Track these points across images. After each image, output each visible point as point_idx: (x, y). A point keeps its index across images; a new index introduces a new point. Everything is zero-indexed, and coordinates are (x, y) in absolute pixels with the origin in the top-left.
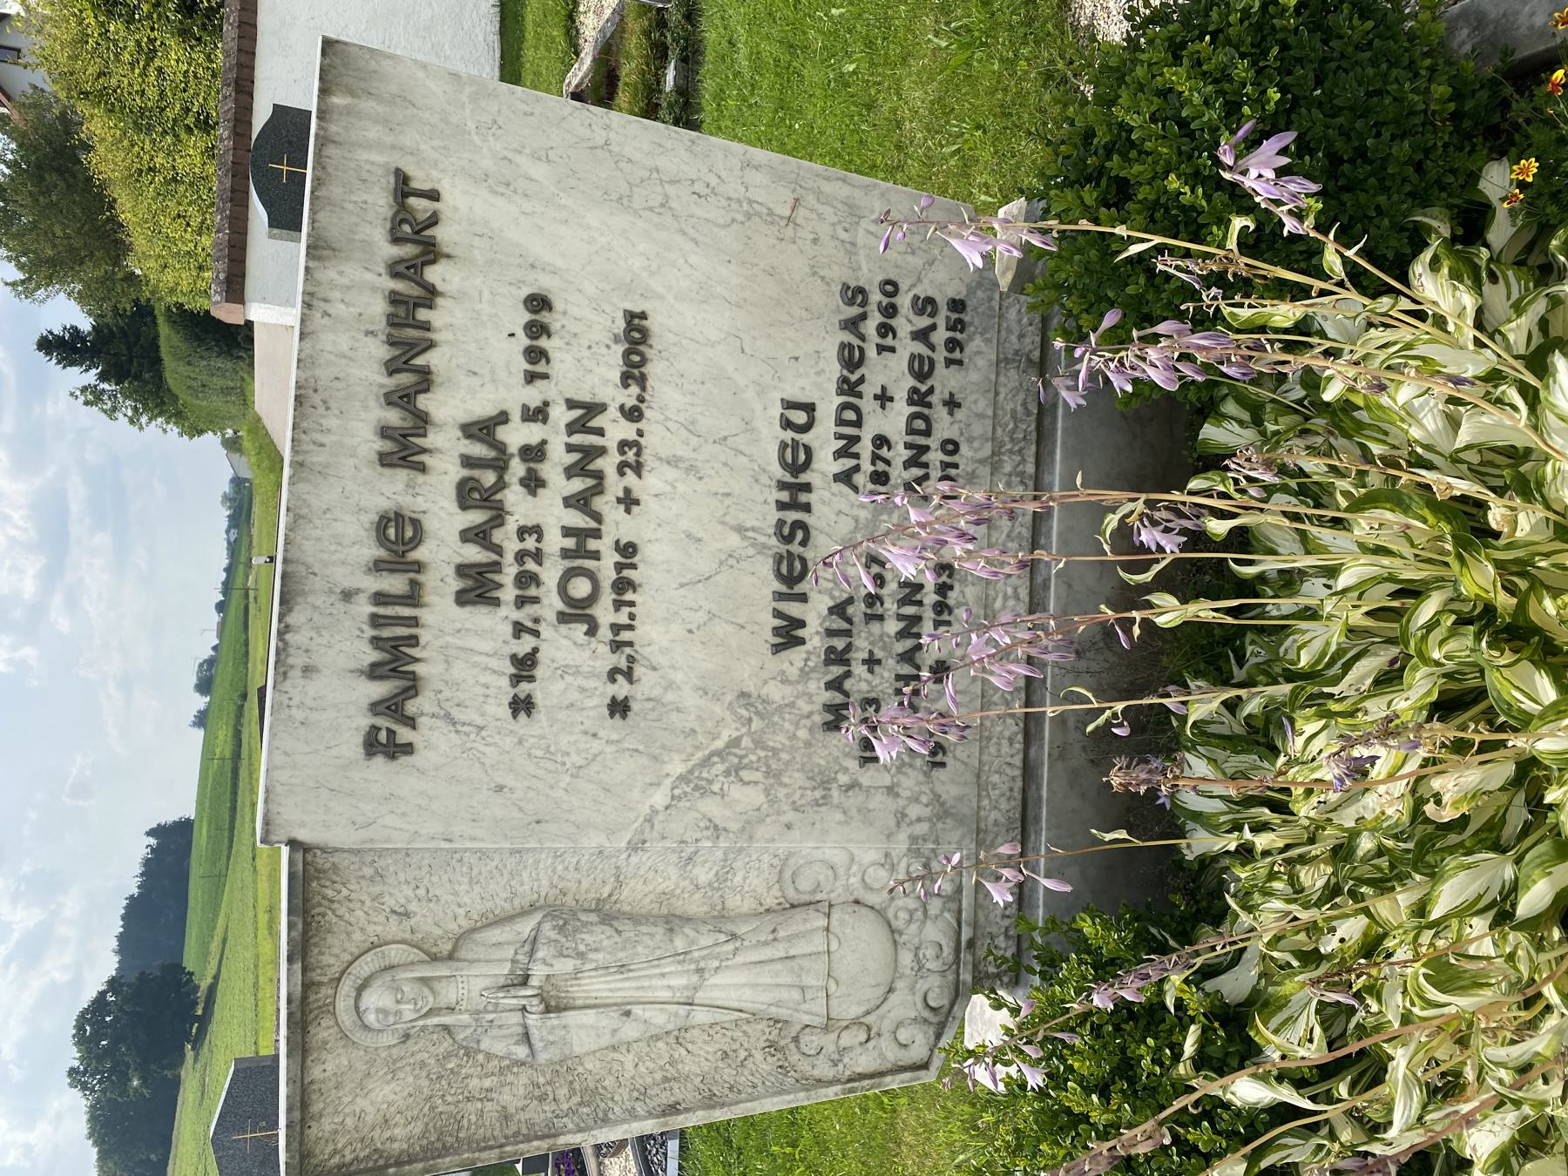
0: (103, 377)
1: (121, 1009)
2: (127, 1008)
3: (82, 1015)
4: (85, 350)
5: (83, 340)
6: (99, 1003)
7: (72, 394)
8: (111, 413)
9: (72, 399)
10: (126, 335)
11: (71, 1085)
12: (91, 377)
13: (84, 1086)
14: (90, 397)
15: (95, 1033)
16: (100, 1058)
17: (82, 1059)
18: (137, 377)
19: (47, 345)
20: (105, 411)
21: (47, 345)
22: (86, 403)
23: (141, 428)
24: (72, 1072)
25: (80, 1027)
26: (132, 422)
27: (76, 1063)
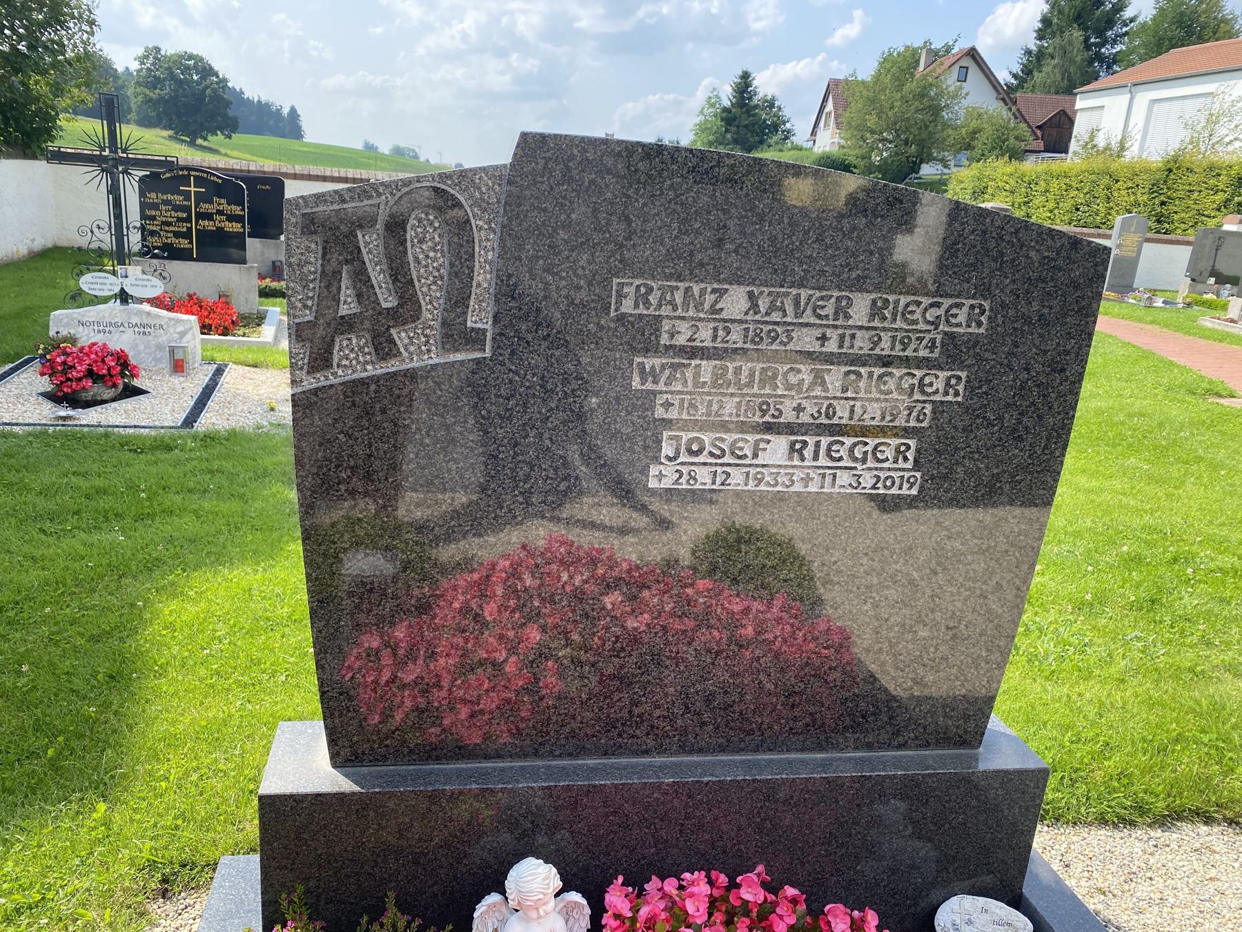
0: (725, 110)
1: (207, 87)
2: (208, 91)
3: (202, 59)
4: (743, 98)
5: (750, 99)
6: (207, 71)
7: (714, 89)
8: (702, 112)
9: (711, 89)
10: (754, 124)
11: (147, 50)
12: (727, 103)
13: (147, 57)
14: (713, 101)
15: (188, 68)
16: (169, 69)
17: (165, 57)
18: (727, 131)
19: (746, 76)
20: (703, 109)
21: (746, 76)
22: (710, 98)
23: (692, 130)
24: (158, 50)
25: (191, 57)
26: (696, 125)
27: (163, 52)
